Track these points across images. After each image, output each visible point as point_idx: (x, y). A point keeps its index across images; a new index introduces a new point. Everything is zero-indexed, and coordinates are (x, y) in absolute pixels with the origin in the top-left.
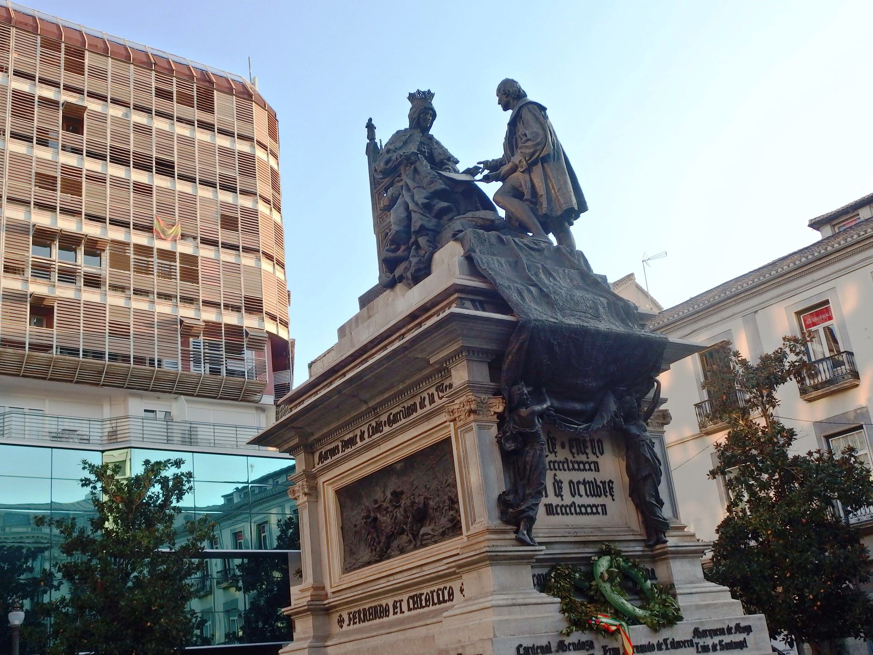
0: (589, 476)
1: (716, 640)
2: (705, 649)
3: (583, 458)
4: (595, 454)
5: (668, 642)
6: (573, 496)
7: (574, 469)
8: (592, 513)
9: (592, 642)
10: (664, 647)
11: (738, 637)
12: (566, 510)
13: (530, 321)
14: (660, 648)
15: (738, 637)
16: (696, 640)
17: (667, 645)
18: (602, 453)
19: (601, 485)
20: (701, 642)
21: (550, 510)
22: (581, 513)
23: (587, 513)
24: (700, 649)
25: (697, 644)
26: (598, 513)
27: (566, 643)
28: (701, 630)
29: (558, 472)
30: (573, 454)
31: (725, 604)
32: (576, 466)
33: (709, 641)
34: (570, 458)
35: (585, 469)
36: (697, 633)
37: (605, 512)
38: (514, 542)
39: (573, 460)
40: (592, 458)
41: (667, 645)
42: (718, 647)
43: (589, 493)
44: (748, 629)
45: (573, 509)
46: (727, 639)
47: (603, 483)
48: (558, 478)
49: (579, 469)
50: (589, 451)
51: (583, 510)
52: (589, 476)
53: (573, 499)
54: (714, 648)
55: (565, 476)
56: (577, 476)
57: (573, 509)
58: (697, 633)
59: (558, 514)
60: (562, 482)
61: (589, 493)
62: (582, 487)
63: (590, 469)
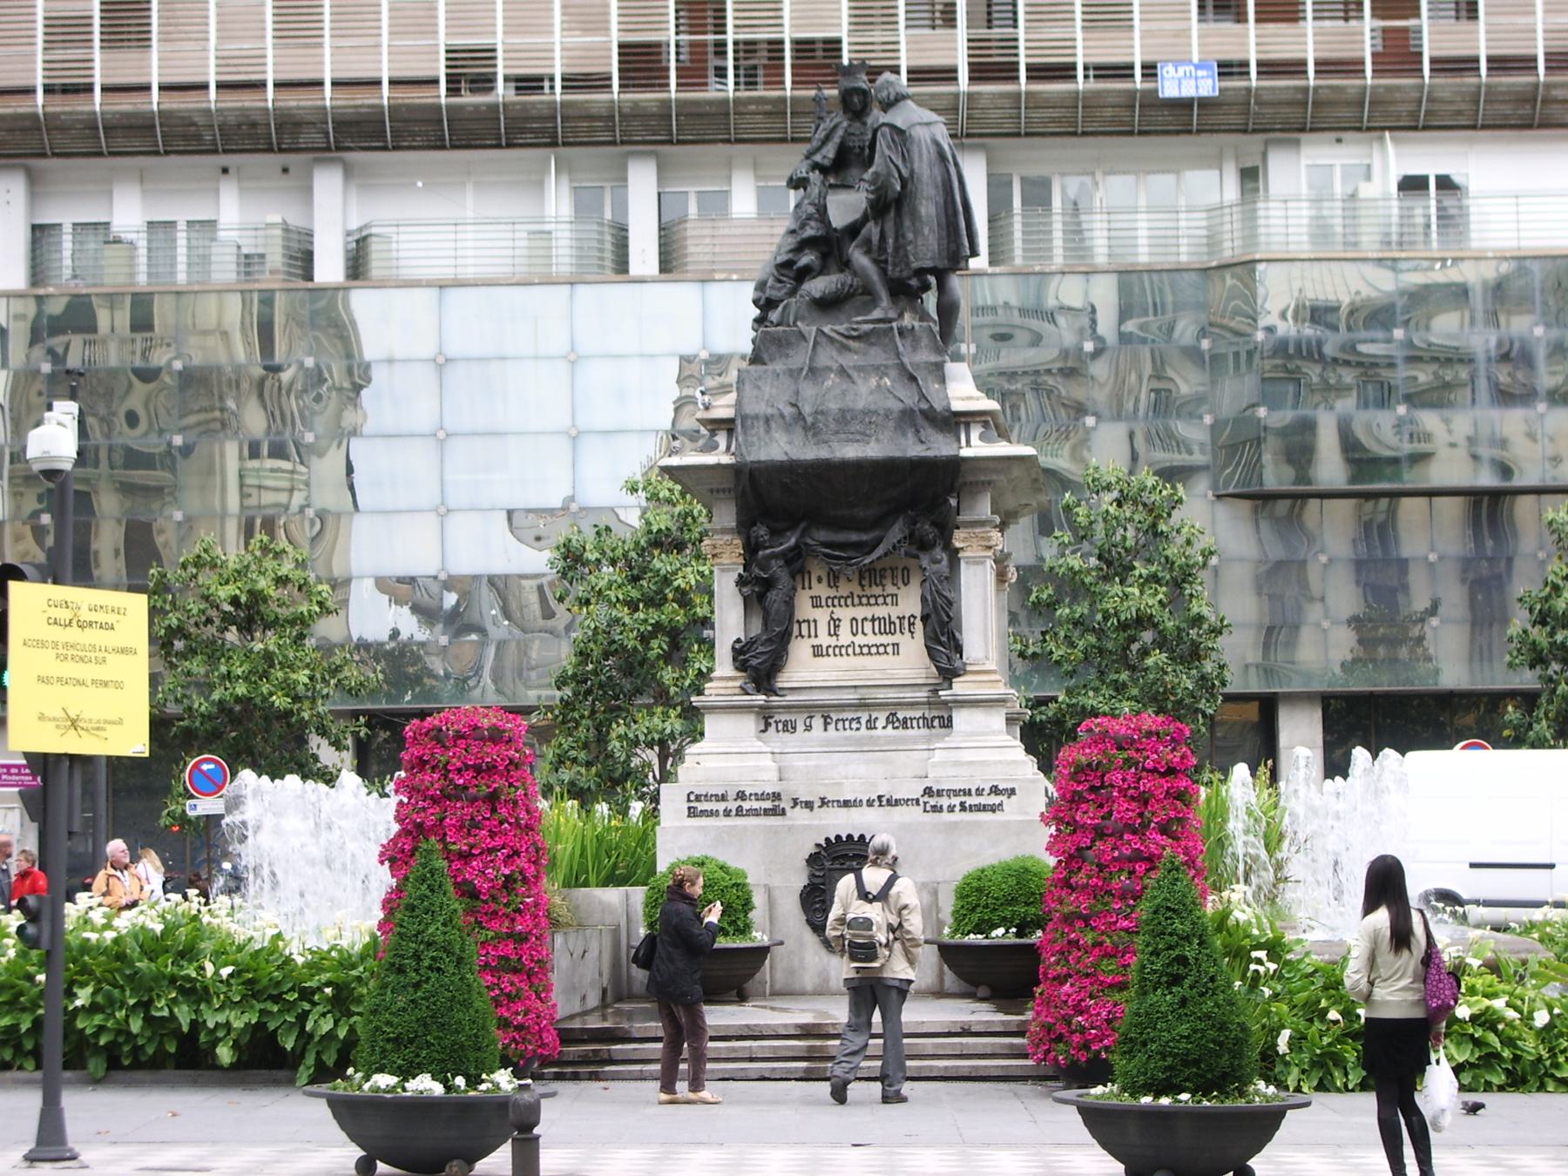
0: (881, 611)
1: (956, 801)
2: (937, 809)
3: (877, 590)
4: (894, 584)
5: (884, 799)
6: (854, 635)
7: (861, 604)
8: (878, 653)
9: (779, 794)
10: (876, 803)
11: (995, 800)
12: (839, 650)
13: (745, 464)
14: (870, 803)
15: (995, 800)
16: (926, 799)
17: (880, 801)
18: (905, 585)
19: (897, 622)
20: (932, 801)
21: (818, 652)
22: (862, 653)
23: (870, 653)
24: (928, 808)
25: (925, 803)
26: (886, 652)
27: (747, 793)
28: (935, 789)
29: (835, 610)
30: (862, 586)
31: (1014, 762)
32: (864, 600)
33: (945, 802)
34: (858, 591)
35: (877, 604)
36: (928, 791)
37: (896, 651)
38: (737, 691)
39: (861, 593)
40: (890, 589)
41: (880, 801)
42: (958, 808)
43: (877, 630)
44: (1012, 792)
45: (850, 650)
46: (971, 801)
47: (901, 619)
48: (835, 617)
49: (869, 604)
50: (888, 582)
51: (865, 650)
52: (881, 611)
53: (852, 638)
54: (951, 809)
55: (845, 614)
56: (861, 612)
57: (850, 650)
58: (928, 791)
59: (828, 655)
60: (839, 620)
61: (877, 630)
62: (868, 626)
63: (885, 603)
